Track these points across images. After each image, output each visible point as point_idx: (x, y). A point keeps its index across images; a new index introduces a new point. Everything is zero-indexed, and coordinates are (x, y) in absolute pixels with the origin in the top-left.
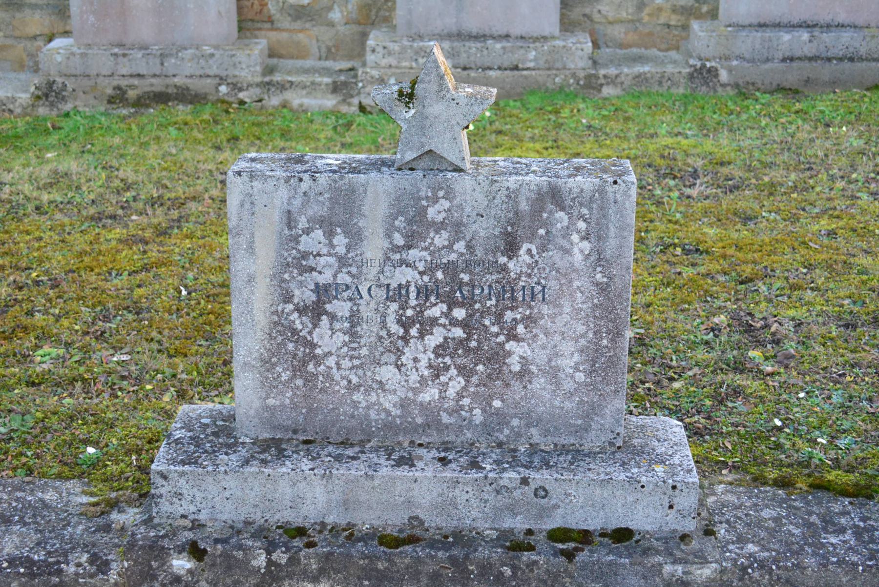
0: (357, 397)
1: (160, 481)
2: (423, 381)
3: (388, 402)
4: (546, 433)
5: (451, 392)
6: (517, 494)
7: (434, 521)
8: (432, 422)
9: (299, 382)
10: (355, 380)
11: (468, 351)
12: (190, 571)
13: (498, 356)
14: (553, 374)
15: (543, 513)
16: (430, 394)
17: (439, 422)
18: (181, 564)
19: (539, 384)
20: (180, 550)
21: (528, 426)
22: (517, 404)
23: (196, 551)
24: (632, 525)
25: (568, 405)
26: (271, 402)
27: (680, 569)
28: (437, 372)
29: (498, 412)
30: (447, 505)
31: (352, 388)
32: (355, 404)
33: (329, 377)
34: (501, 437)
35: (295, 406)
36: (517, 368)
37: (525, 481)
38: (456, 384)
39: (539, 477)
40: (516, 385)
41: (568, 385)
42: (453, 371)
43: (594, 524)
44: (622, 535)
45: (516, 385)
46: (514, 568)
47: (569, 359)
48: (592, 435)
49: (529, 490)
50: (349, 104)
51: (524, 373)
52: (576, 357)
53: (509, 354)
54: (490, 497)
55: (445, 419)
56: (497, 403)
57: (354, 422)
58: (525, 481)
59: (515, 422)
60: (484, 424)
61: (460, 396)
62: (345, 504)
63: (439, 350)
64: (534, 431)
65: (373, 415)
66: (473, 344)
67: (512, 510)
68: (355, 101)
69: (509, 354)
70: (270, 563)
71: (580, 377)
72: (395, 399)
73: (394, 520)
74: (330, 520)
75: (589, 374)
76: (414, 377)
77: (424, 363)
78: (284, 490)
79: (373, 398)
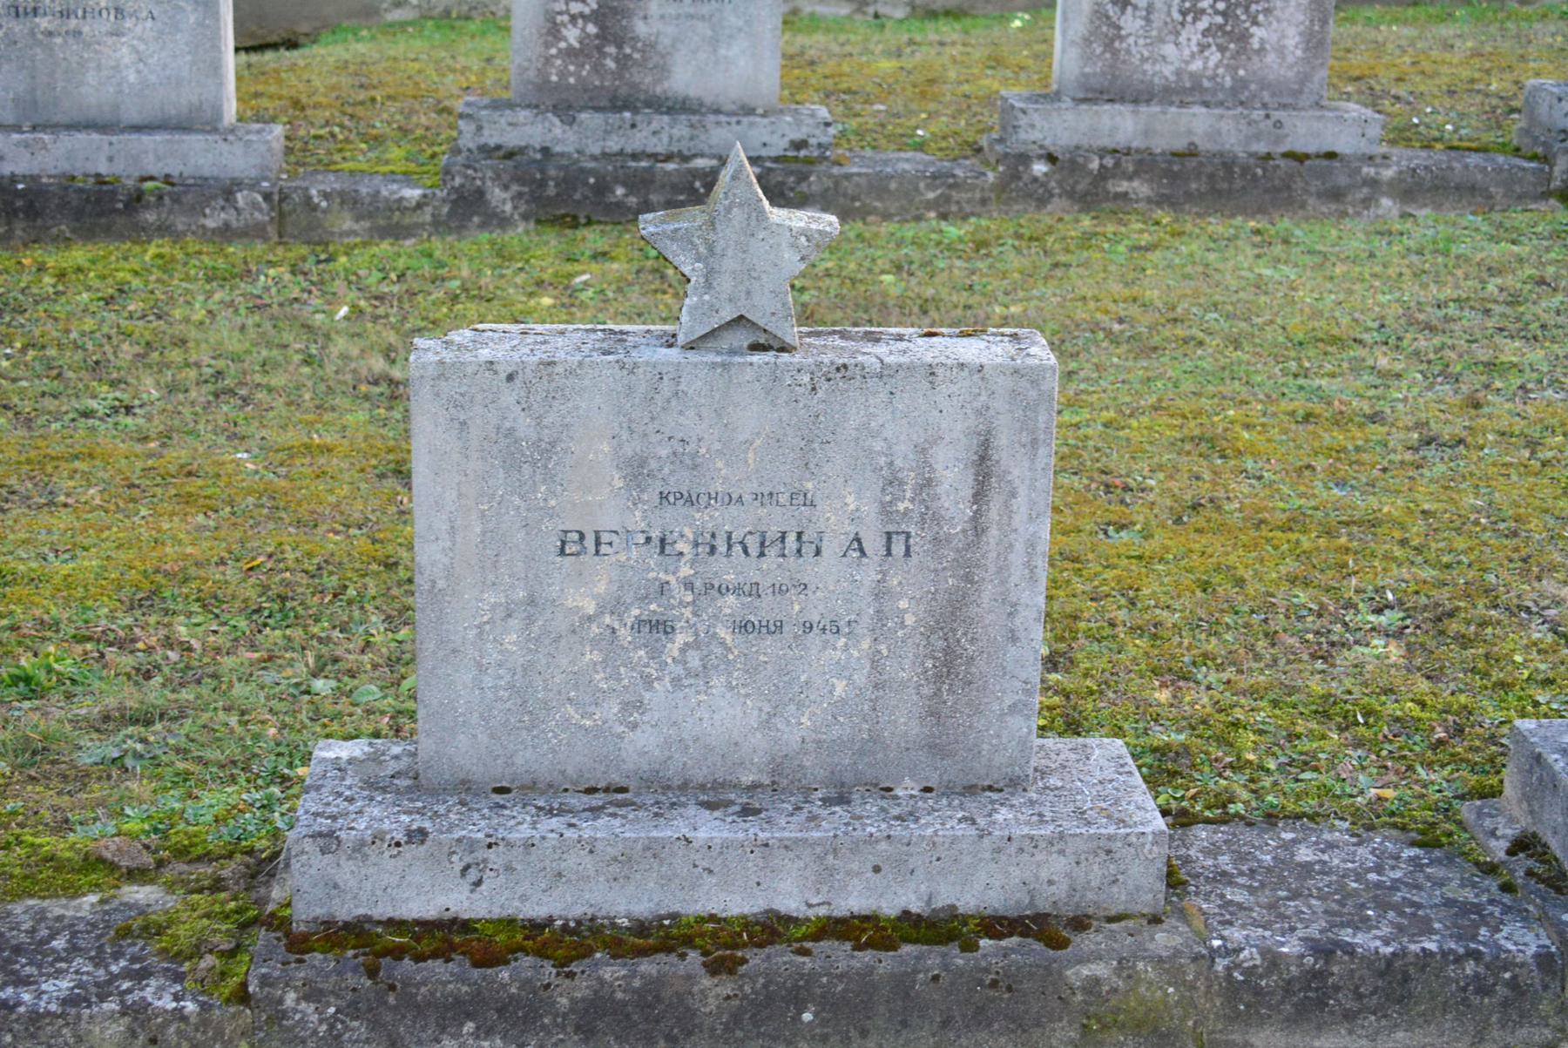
0: (1147, 66)
1: (1021, 115)
2: (1193, 55)
3: (1168, 71)
4: (1273, 95)
5: (1211, 64)
6: (1262, 126)
7: (1204, 145)
8: (1197, 87)
9: (1108, 55)
10: (1146, 54)
11: (1225, 33)
12: (1046, 174)
13: (1244, 37)
14: (1281, 51)
15: (1278, 140)
16: (1196, 66)
17: (1201, 86)
18: (1040, 168)
19: (1271, 58)
20: (1040, 157)
21: (1262, 89)
22: (1254, 72)
23: (1051, 158)
24: (1338, 149)
25: (1290, 74)
26: (1087, 70)
27: (1372, 171)
28: (1203, 48)
29: (1242, 80)
30: (1215, 134)
31: (1144, 60)
32: (1145, 72)
33: (1128, 52)
34: (1243, 98)
35: (1103, 73)
36: (1256, 46)
37: (1268, 116)
38: (1214, 57)
39: (1276, 115)
40: (1255, 59)
41: (1290, 59)
42: (1214, 48)
43: (1312, 149)
44: (1331, 156)
45: (1255, 59)
46: (1265, 170)
47: (1292, 40)
48: (1304, 97)
49: (1270, 123)
50: (864, 13)
51: (1261, 51)
52: (1297, 39)
53: (1252, 36)
54: (1243, 127)
55: (1206, 84)
56: (1241, 72)
57: (1142, 87)
58: (1268, 116)
59: (1253, 87)
60: (1232, 88)
61: (1217, 66)
62: (1147, 133)
63: (1206, 33)
64: (1265, 94)
65: (1156, 80)
66: (1228, 28)
67: (1257, 137)
68: (871, 10)
69: (1252, 36)
70: (1102, 166)
71: (1299, 53)
72: (1172, 68)
73: (1180, 144)
74: (1135, 145)
75: (1306, 50)
76: (1187, 52)
77: (1194, 42)
78: (1106, 122)
79: (1157, 68)
